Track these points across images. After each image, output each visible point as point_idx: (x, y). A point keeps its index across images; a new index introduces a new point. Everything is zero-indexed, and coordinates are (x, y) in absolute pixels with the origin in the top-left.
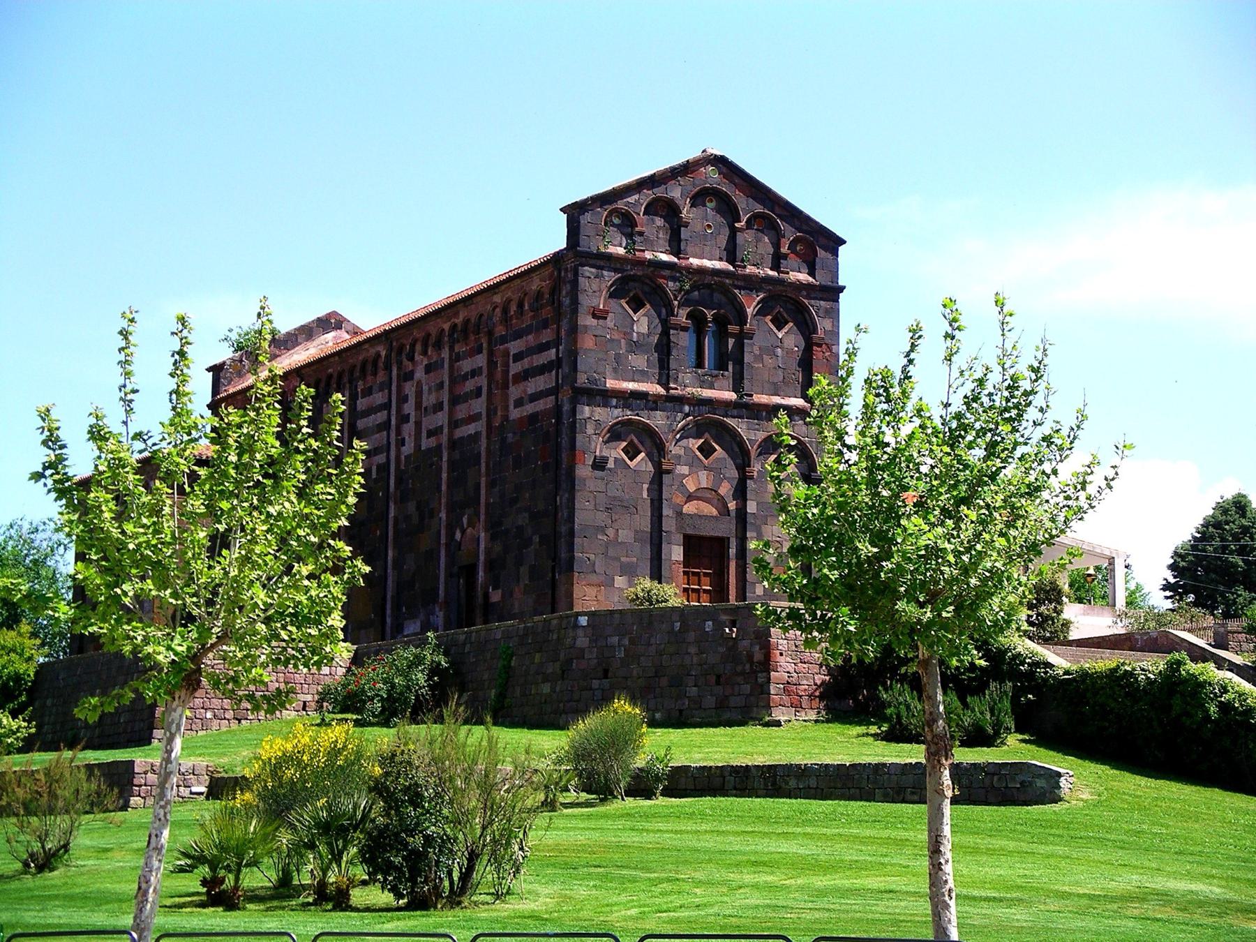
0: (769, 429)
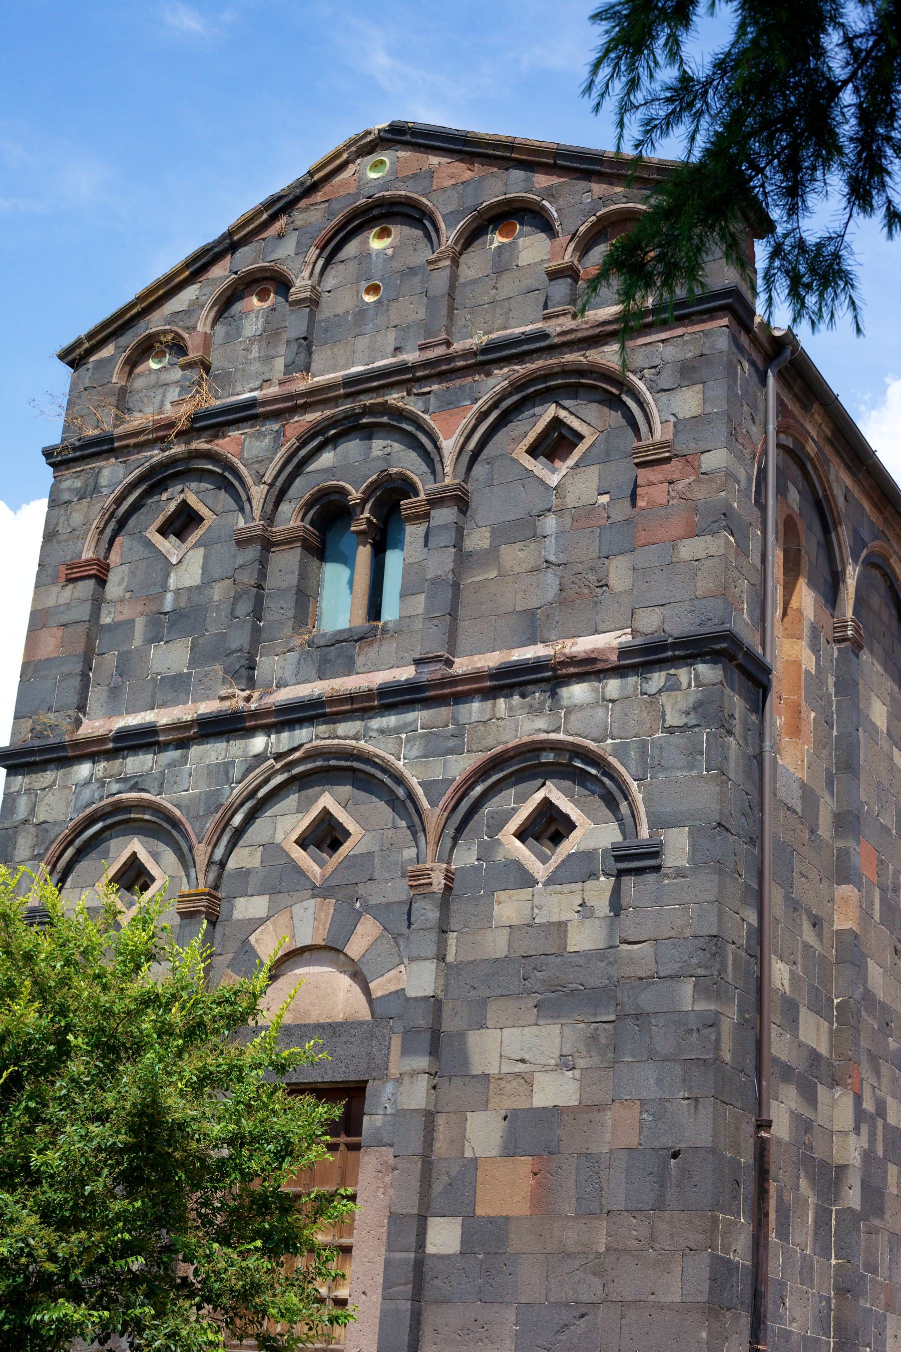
0: (490, 741)
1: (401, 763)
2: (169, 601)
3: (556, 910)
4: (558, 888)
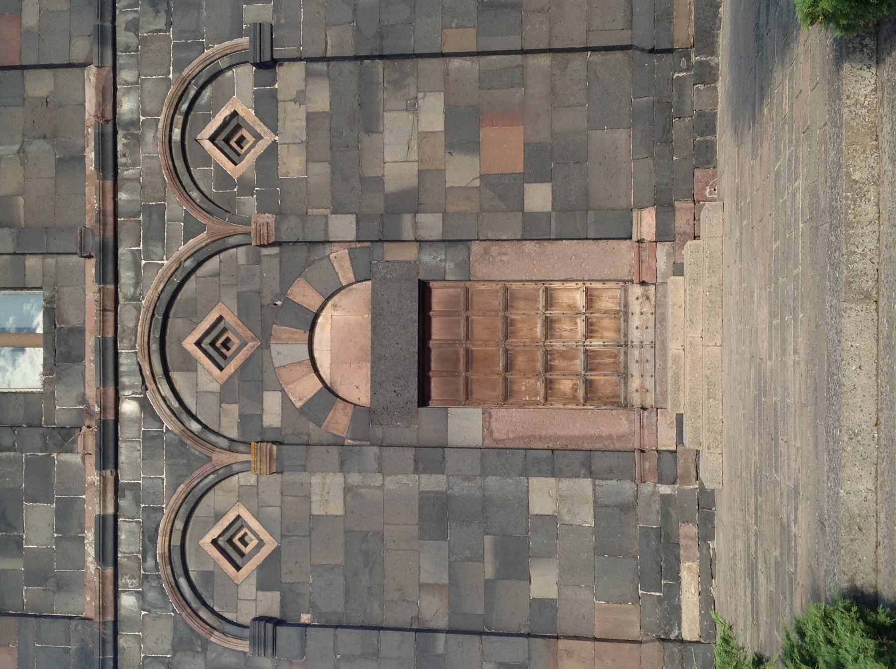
1: (165, 262)
3: (298, 123)
4: (280, 123)
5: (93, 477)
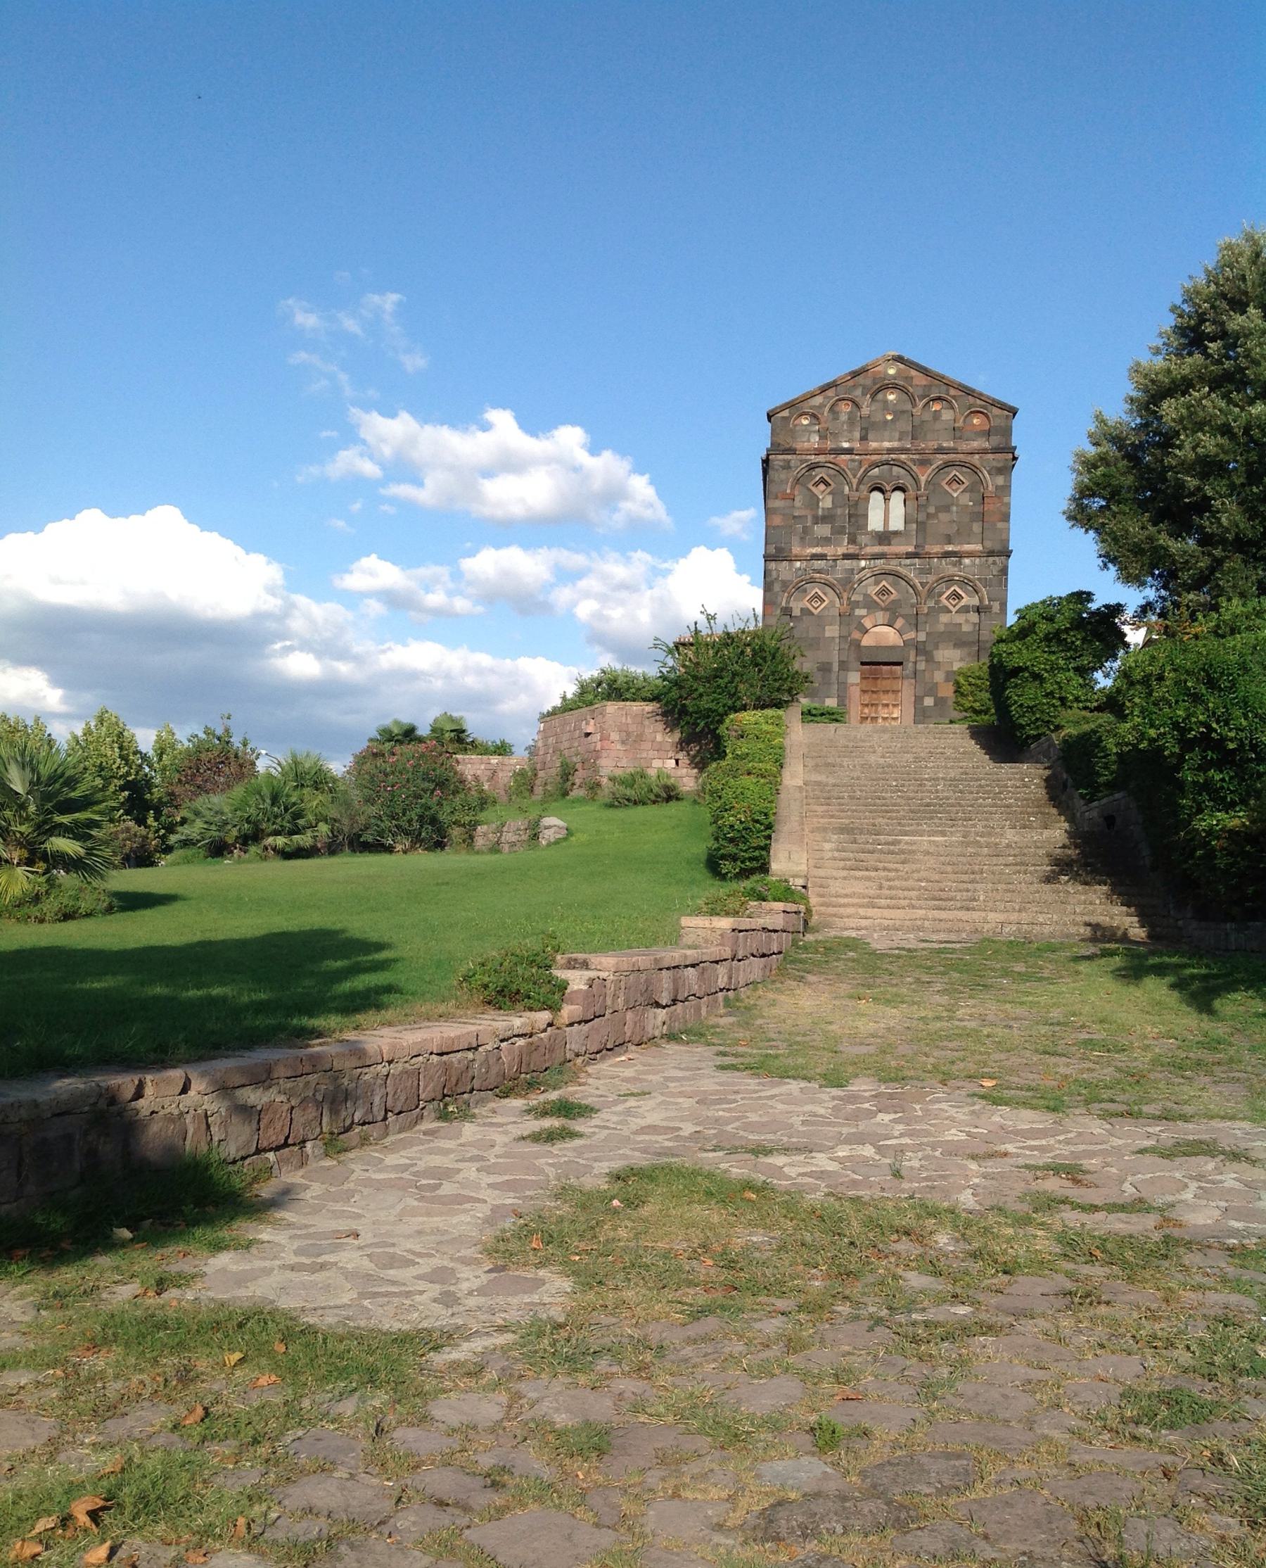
2: (820, 512)
5: (840, 551)
